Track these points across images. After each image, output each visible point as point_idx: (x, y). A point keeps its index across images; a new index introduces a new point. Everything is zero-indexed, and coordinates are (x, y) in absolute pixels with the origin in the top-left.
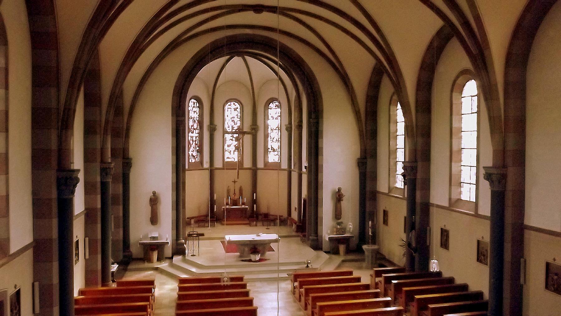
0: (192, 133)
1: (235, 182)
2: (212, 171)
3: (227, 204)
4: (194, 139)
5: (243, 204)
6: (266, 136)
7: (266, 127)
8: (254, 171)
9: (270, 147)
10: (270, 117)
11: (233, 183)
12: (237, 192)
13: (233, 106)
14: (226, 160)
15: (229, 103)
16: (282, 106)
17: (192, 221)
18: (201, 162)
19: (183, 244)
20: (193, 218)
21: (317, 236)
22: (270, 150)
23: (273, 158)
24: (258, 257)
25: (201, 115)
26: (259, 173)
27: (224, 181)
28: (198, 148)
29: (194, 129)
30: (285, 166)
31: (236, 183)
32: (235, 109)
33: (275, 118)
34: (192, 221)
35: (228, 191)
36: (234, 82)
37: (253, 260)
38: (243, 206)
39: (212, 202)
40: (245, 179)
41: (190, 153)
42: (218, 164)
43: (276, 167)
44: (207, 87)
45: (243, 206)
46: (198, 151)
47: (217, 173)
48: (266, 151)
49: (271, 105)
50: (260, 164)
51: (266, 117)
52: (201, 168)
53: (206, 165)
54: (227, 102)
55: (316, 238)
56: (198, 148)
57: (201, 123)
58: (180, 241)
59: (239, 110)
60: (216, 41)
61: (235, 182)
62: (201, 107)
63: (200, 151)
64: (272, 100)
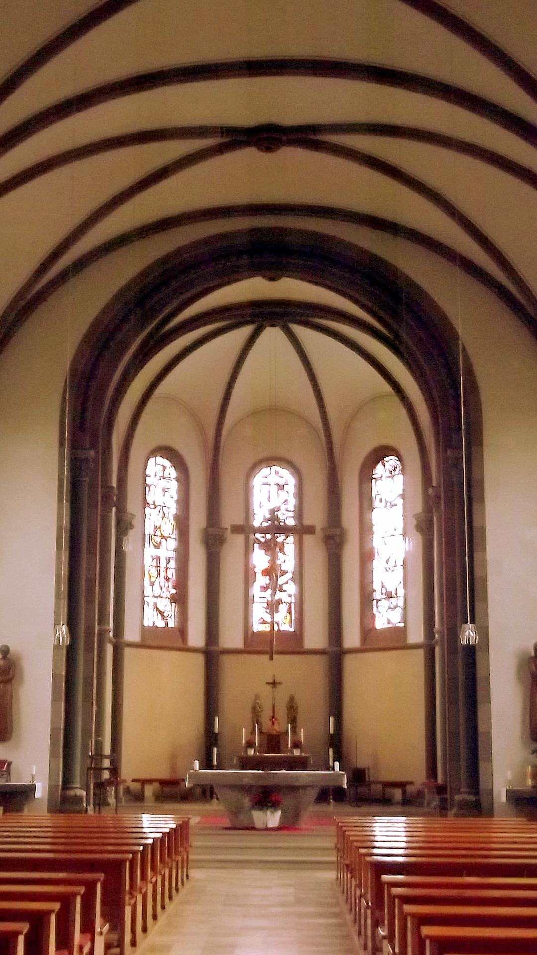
0: (158, 546)
1: (274, 684)
2: (212, 657)
3: (250, 744)
4: (163, 563)
5: (296, 745)
6: (367, 557)
7: (366, 529)
8: (335, 657)
9: (377, 586)
10: (377, 504)
11: (269, 688)
12: (282, 713)
13: (274, 479)
14: (257, 627)
15: (265, 471)
16: (407, 467)
17: (149, 791)
18: (182, 630)
19: (78, 800)
20: (150, 782)
21: (477, 793)
22: (377, 596)
23: (386, 616)
24: (273, 818)
25: (184, 502)
26: (350, 663)
27: (244, 681)
28: (174, 591)
29: (163, 538)
30: (416, 635)
31: (279, 688)
32: (281, 488)
33: (391, 507)
34: (149, 791)
35: (256, 712)
36: (273, 412)
37: (258, 824)
38: (297, 752)
39: (211, 738)
40: (304, 678)
41: (149, 600)
42: (231, 638)
43: (395, 640)
44: (201, 429)
45: (297, 752)
46: (174, 599)
47: (230, 667)
48: (367, 600)
49: (379, 470)
50: (352, 638)
51: (366, 502)
52: (181, 645)
53: (197, 637)
54: (255, 466)
55: (472, 798)
56: (174, 591)
57: (182, 524)
58: (72, 793)
59: (291, 487)
60: (178, 252)
61: (274, 684)
62: (184, 479)
63: (180, 599)
64: (379, 454)
